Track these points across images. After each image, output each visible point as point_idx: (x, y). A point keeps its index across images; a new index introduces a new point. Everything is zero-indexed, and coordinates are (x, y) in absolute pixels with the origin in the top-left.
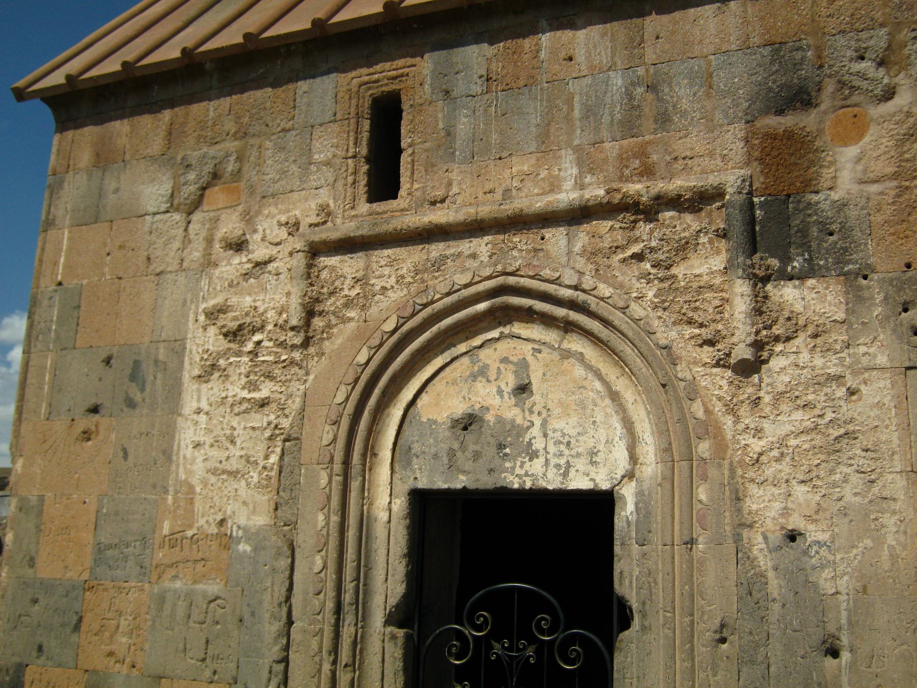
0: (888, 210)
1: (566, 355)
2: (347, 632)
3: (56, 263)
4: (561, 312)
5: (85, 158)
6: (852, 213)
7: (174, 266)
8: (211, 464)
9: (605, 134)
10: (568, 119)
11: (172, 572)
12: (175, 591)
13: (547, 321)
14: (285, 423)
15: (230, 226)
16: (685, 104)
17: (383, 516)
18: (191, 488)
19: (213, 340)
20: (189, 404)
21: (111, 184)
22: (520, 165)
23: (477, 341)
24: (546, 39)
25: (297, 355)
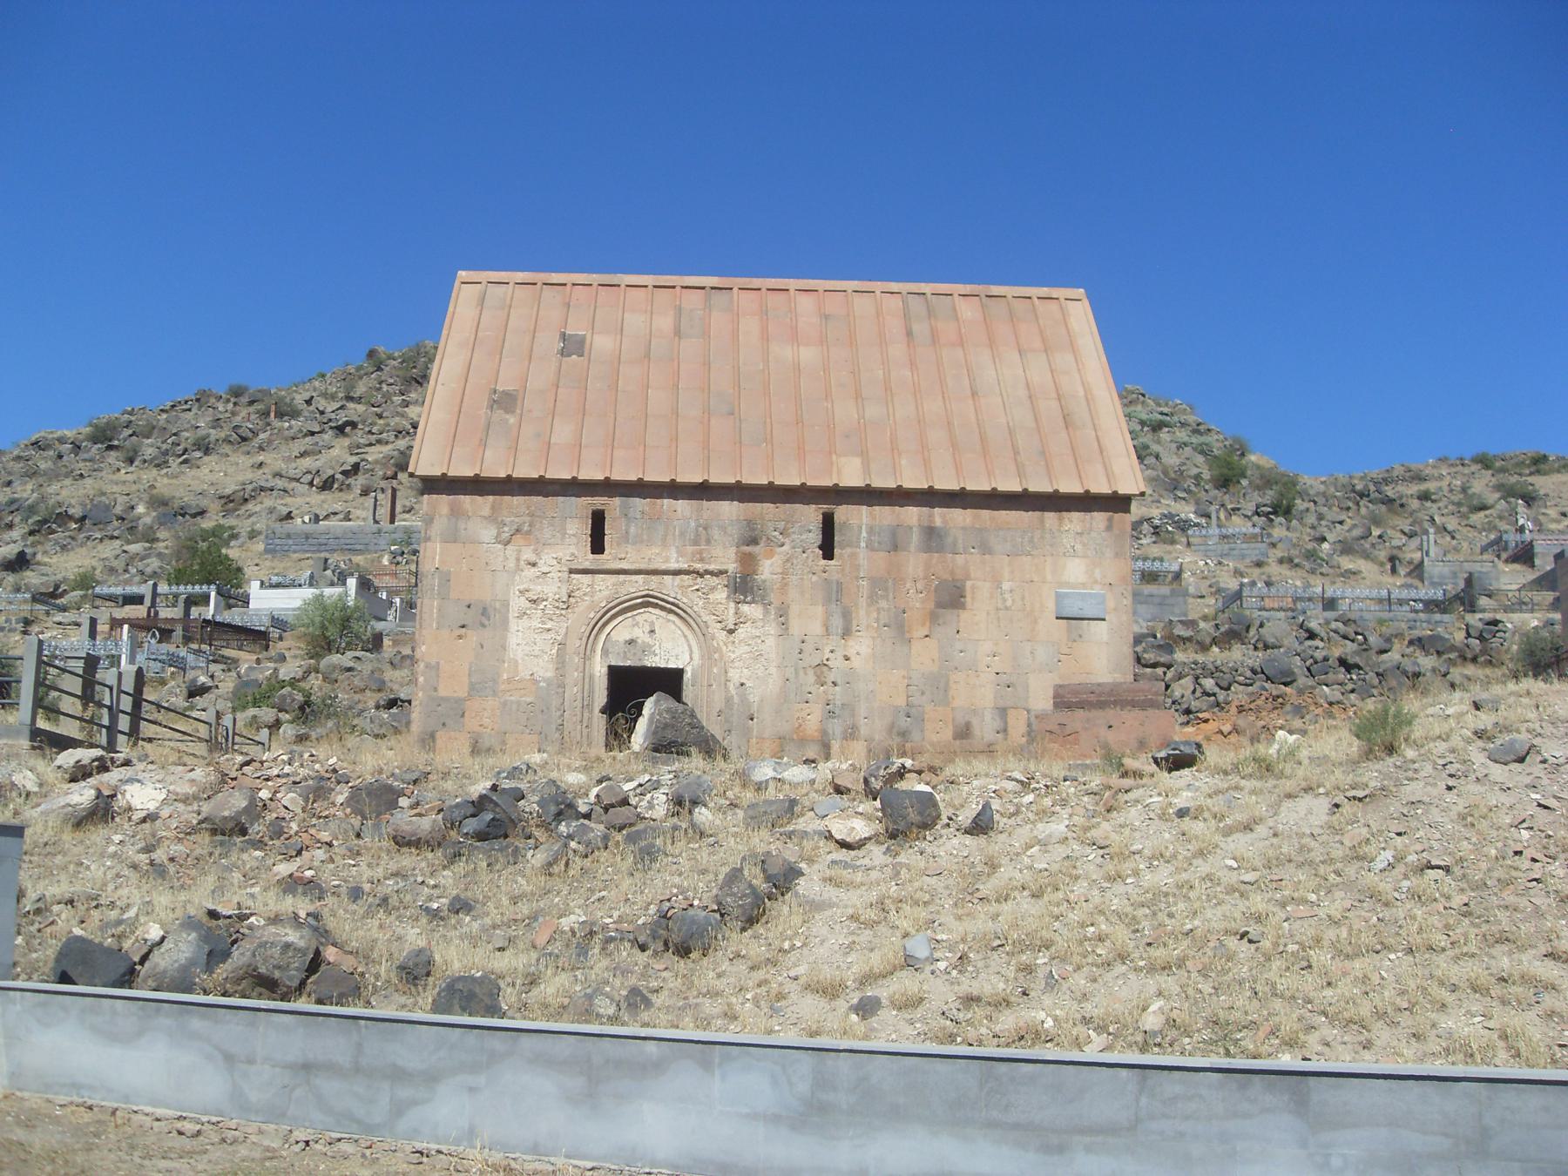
0: (778, 585)
1: (669, 620)
2: (586, 715)
3: (434, 558)
4: (668, 606)
5: (445, 510)
6: (768, 583)
7: (501, 568)
8: (526, 652)
9: (687, 543)
10: (674, 534)
11: (509, 694)
12: (512, 702)
13: (663, 608)
14: (559, 638)
15: (528, 554)
16: (716, 537)
17: (598, 674)
18: (517, 661)
19: (523, 603)
21: (462, 525)
23: (635, 613)
24: (666, 501)
25: (563, 612)
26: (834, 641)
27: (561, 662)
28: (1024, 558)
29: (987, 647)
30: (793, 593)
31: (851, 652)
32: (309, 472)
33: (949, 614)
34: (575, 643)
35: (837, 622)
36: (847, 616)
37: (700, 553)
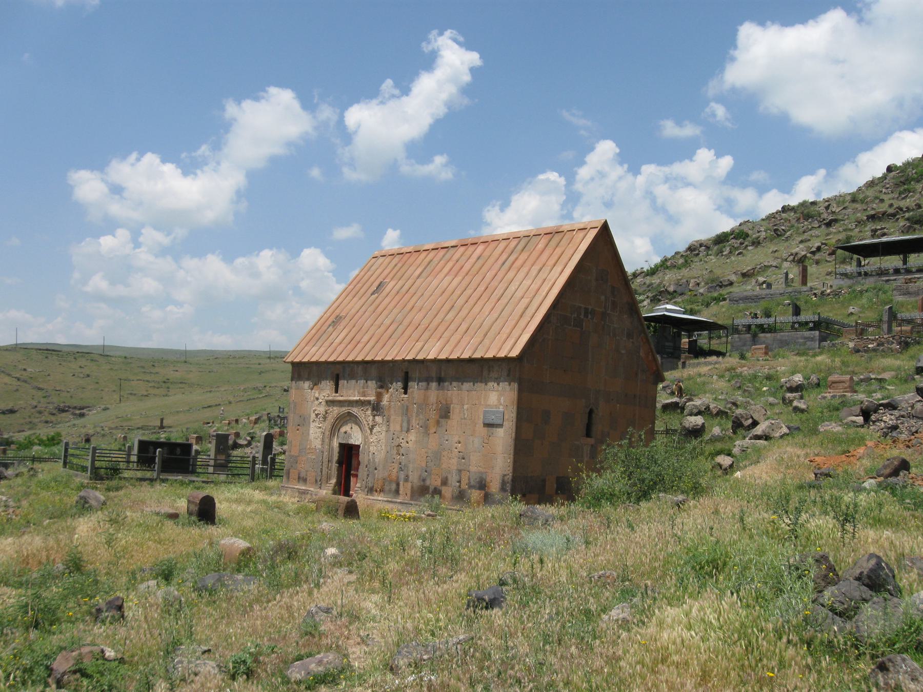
20: (311, 426)
22: (351, 391)
26: (404, 435)
27: (323, 441)
28: (474, 392)
29: (456, 439)
30: (392, 412)
31: (409, 440)
32: (792, 255)
33: (443, 421)
34: (327, 433)
35: (405, 425)
36: (409, 422)
37: (364, 392)
